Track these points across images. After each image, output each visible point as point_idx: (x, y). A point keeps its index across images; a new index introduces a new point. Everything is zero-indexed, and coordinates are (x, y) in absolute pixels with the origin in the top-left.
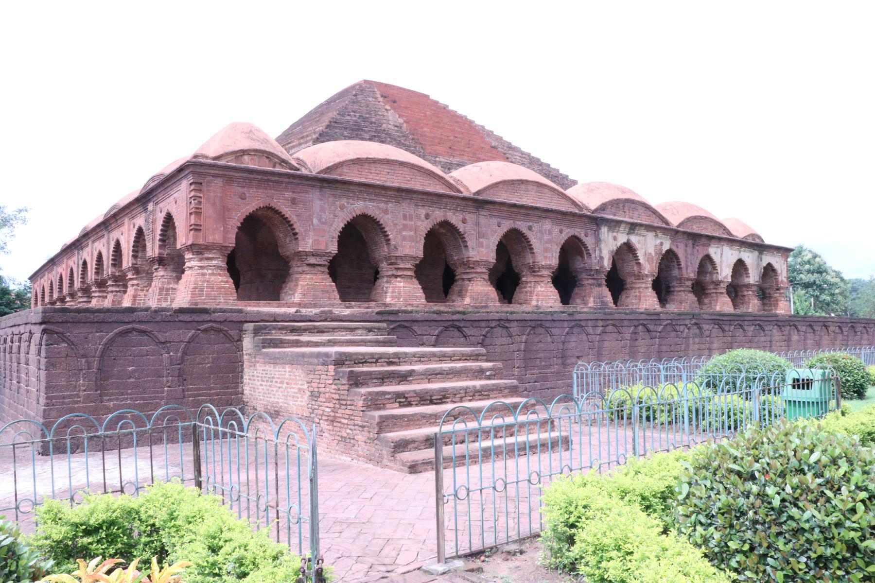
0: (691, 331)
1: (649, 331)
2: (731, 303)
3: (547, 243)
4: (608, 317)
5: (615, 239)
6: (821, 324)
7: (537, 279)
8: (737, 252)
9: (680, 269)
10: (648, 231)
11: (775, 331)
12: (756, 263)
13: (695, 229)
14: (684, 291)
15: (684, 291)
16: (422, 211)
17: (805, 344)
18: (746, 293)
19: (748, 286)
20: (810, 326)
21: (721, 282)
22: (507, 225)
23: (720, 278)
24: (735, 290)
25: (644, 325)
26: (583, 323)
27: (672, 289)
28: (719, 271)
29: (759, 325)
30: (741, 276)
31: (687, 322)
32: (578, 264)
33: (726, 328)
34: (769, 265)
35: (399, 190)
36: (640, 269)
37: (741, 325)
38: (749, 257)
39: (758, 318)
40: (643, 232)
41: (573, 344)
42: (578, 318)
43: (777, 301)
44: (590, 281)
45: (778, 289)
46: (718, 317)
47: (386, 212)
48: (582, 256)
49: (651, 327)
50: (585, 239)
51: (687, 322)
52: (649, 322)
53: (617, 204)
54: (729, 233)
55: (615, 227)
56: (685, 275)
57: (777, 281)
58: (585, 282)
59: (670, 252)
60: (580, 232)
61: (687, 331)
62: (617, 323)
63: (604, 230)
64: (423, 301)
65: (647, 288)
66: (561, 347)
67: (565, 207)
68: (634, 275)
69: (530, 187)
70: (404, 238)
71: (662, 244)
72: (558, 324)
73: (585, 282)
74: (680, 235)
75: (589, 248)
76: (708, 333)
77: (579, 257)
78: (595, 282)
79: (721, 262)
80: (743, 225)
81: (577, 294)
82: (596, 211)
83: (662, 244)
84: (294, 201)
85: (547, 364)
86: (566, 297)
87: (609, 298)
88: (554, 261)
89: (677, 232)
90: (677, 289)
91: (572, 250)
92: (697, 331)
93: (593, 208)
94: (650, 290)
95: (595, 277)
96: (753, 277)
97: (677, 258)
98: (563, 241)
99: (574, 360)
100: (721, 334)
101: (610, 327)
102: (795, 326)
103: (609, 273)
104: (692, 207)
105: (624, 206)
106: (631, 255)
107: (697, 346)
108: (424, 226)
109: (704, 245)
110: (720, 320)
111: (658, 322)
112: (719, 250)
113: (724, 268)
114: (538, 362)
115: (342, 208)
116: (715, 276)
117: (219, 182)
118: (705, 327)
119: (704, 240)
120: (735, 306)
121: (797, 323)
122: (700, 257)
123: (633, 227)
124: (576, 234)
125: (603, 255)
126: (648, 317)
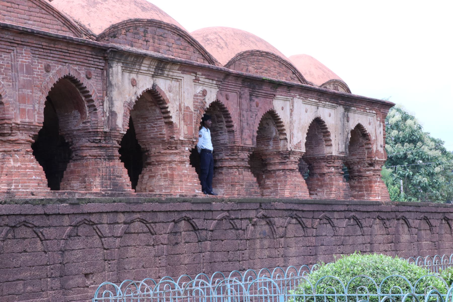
0: (258, 228)
1: (195, 229)
2: (305, 187)
3: (24, 87)
4: (134, 208)
5: (134, 83)
6: (441, 216)
7: (8, 147)
8: (314, 108)
9: (231, 132)
10: (184, 72)
11: (377, 227)
12: (340, 124)
13: (252, 71)
14: (238, 167)
15: (238, 167)
17: (420, 247)
18: (326, 170)
19: (329, 159)
20: (426, 219)
21: (291, 153)
23: (290, 147)
24: (311, 166)
25: (188, 220)
26: (94, 218)
27: (219, 164)
28: (288, 137)
30: (318, 143)
31: (252, 214)
32: (75, 123)
33: (308, 223)
34: (359, 127)
36: (173, 132)
37: (328, 219)
38: (331, 116)
39: (353, 208)
40: (177, 74)
41: (80, 254)
42: (86, 210)
43: (370, 182)
44: (95, 152)
45: (371, 165)
46: (296, 207)
48: (81, 111)
49: (199, 223)
50: (86, 83)
51: (252, 214)
52: (195, 214)
53: (133, 26)
54: (301, 78)
55: (134, 64)
56: (239, 143)
57: (370, 153)
58: (87, 153)
59: (216, 105)
61: (251, 228)
62: (148, 217)
65: (182, 162)
66: (58, 257)
67: (54, 29)
68: (163, 142)
71: (204, 93)
72: (53, 221)
73: (87, 153)
74: (231, 81)
75: (93, 97)
76: (281, 230)
77: (76, 113)
78: (102, 152)
79: (291, 122)
80: (320, 67)
81: (72, 172)
82: (102, 36)
83: (204, 93)
85: (36, 289)
86: (55, 177)
87: (125, 178)
88: (37, 118)
89: (227, 75)
90: (227, 164)
91: (65, 98)
93: (97, 32)
94: (188, 165)
95: (103, 144)
96: (336, 146)
97: (227, 115)
98: (51, 85)
99: (79, 280)
100: (301, 233)
101: (137, 224)
102: (405, 219)
103: (125, 137)
104: (246, 36)
105: (145, 32)
106: (158, 111)
107: (266, 253)
110: (297, 211)
111: (209, 215)
113: (295, 131)
114: (20, 286)
116: (282, 143)
118: (278, 221)
119: (266, 89)
120: (311, 189)
121: (407, 215)
122: (260, 115)
123: (162, 65)
124: (73, 74)
125: (115, 109)
126: (194, 207)
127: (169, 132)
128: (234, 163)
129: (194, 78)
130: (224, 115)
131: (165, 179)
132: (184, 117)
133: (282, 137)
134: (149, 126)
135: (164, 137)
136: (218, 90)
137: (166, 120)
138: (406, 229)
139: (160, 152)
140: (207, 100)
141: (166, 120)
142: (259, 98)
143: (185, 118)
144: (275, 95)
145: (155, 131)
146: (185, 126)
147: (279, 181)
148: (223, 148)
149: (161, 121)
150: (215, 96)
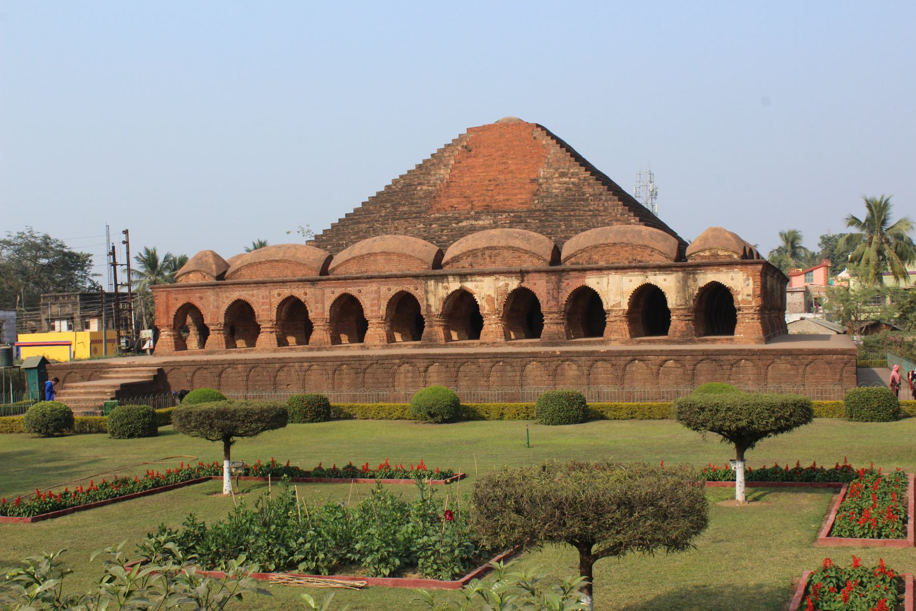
0: (402, 368)
5: (447, 288)
16: (275, 292)
22: (339, 292)
29: (504, 362)
35: (257, 283)
47: (253, 296)
51: (397, 361)
54: (661, 253)
60: (409, 287)
63: (431, 283)
64: (276, 346)
69: (379, 258)
70: (263, 310)
71: (507, 285)
72: (271, 365)
82: (447, 263)
83: (507, 285)
84: (201, 298)
92: (410, 368)
108: (276, 301)
109: (577, 278)
112: (605, 280)
113: (612, 297)
115: (227, 297)
117: (164, 294)
123: (463, 276)
138: (574, 367)
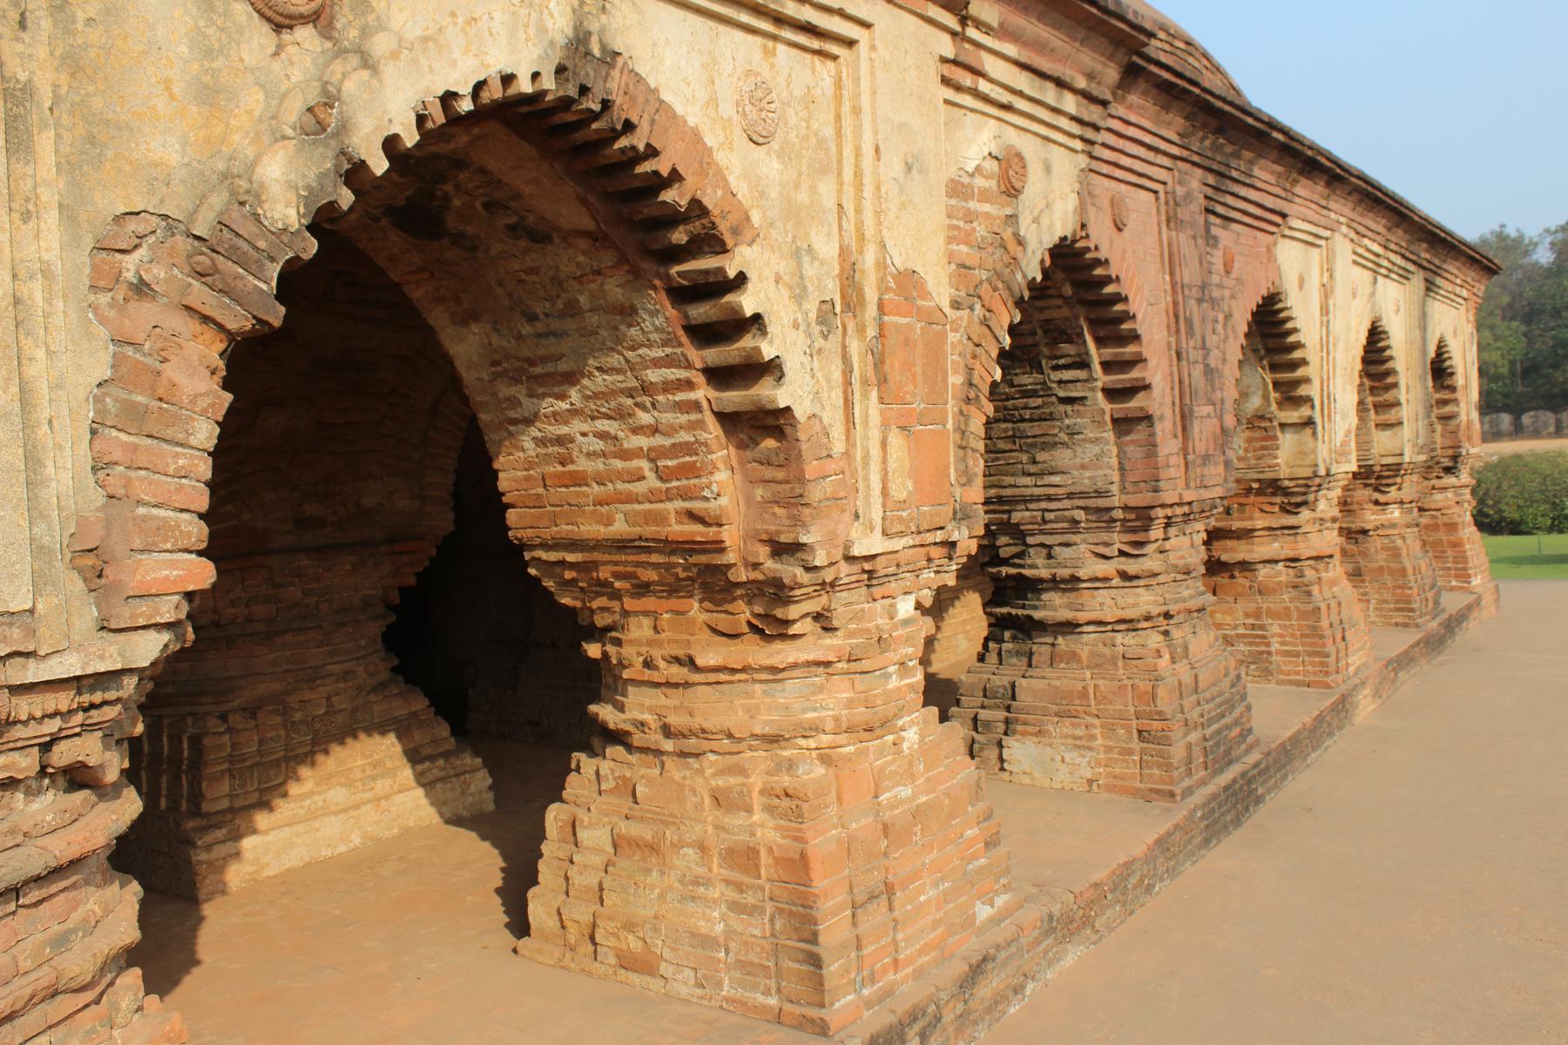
27: (1053, 607)
36: (795, 502)
59: (1069, 260)
68: (714, 584)
71: (1010, 176)
83: (1010, 176)
90: (1102, 604)
106: (658, 315)
127: (759, 492)
128: (1143, 600)
129: (947, 47)
130: (1093, 323)
131: (739, 887)
132: (879, 364)
133: (1293, 416)
134: (598, 445)
135: (718, 547)
136: (1083, 161)
137: (734, 398)
139: (691, 663)
140: (1026, 228)
141: (734, 398)
142: (1234, 226)
143: (893, 367)
144: (1284, 216)
145: (639, 488)
146: (896, 439)
147: (1272, 614)
148: (1080, 515)
149: (681, 407)
150: (1072, 201)
